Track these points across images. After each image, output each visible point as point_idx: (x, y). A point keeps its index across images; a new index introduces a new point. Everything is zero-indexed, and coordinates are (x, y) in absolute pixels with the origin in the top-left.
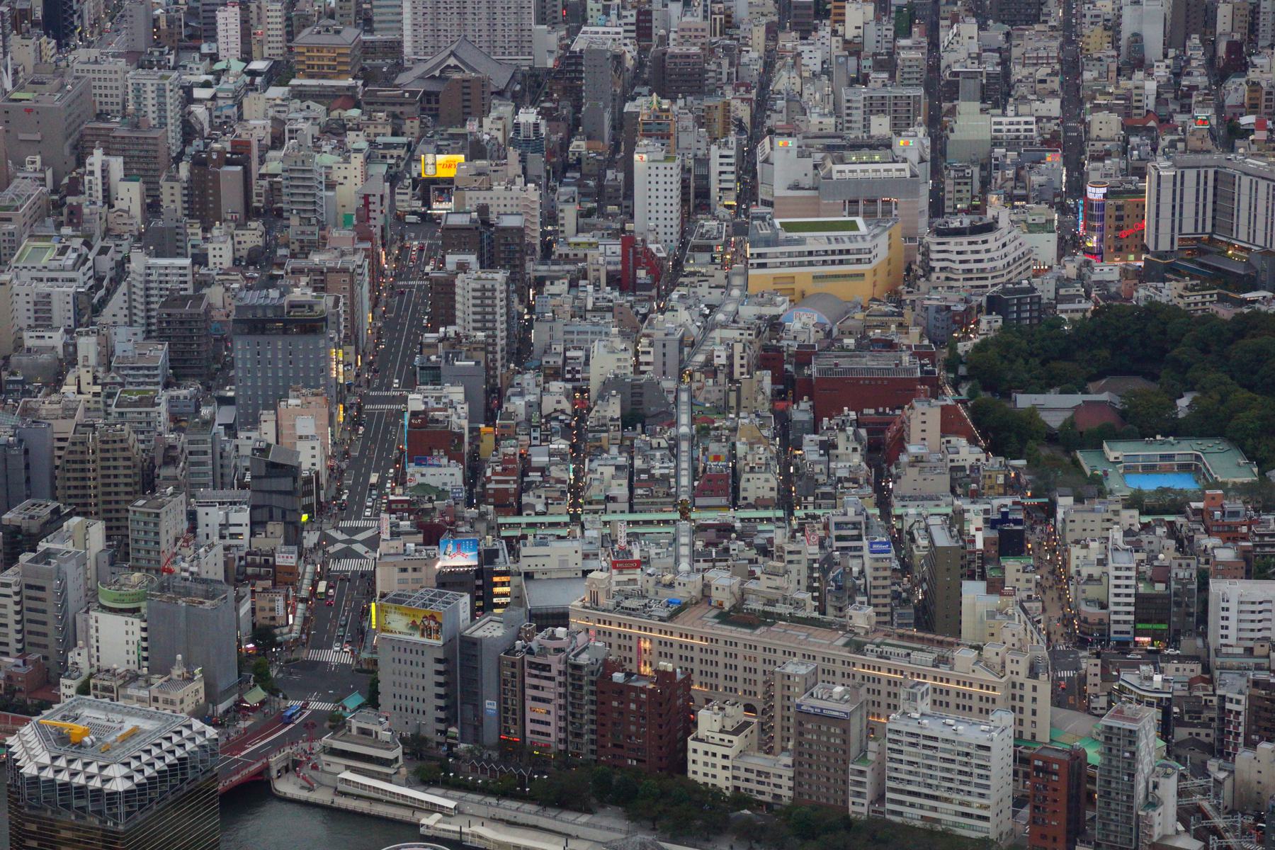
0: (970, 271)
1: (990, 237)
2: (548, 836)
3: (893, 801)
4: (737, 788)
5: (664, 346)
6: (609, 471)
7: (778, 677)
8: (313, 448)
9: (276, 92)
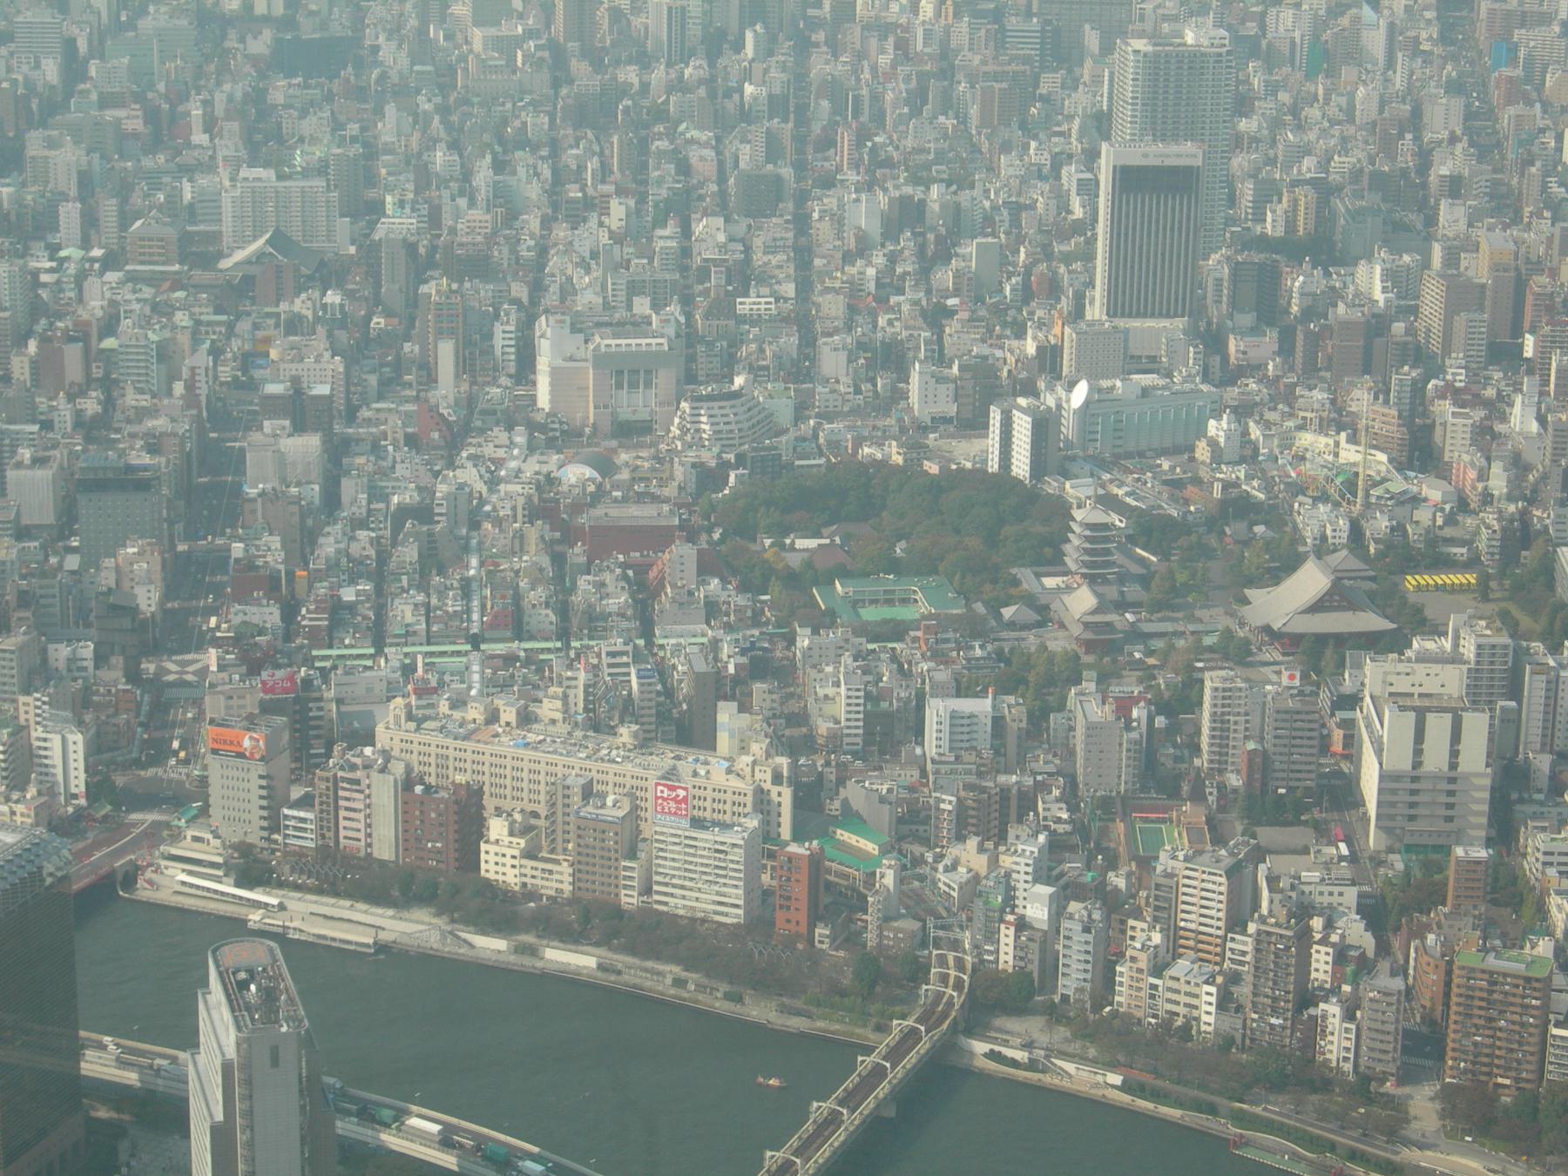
0: (720, 432)
1: (738, 402)
2: (361, 928)
4: (524, 885)
6: (408, 610)
7: (560, 788)
9: (112, 277)
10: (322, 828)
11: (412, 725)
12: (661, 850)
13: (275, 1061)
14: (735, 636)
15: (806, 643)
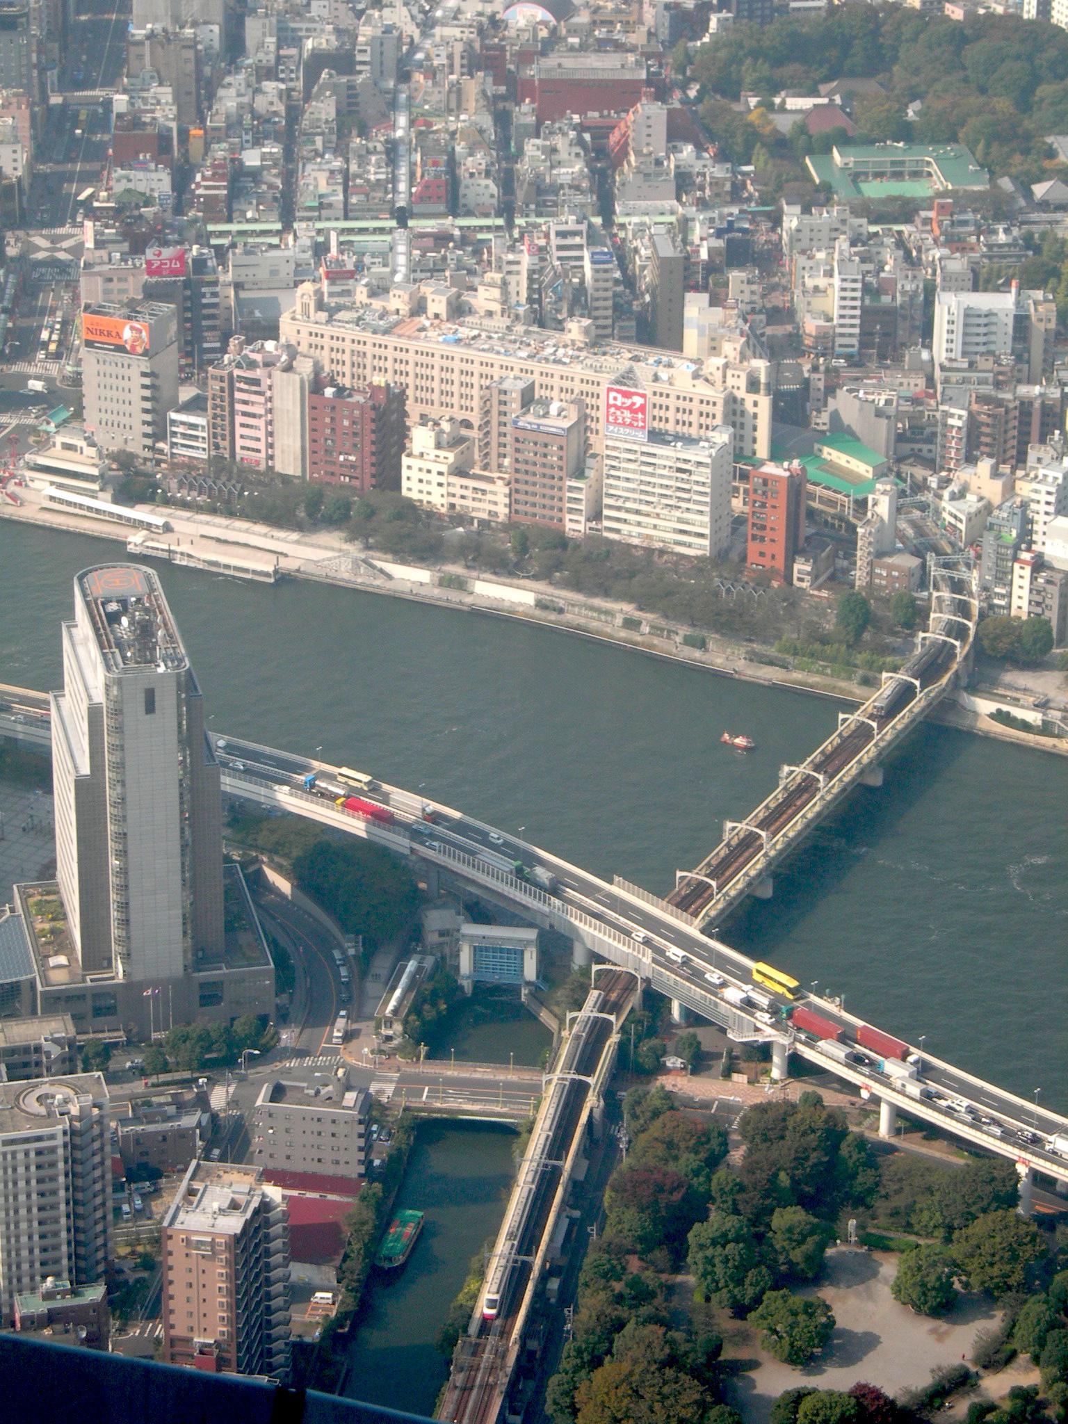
2: (260, 554)
3: (609, 518)
4: (452, 506)
5: (382, 44)
6: (322, 178)
7: (495, 393)
8: (15, 152)
10: (215, 435)
11: (323, 316)
12: (613, 467)
13: (150, 708)
14: (709, 214)
15: (794, 224)
